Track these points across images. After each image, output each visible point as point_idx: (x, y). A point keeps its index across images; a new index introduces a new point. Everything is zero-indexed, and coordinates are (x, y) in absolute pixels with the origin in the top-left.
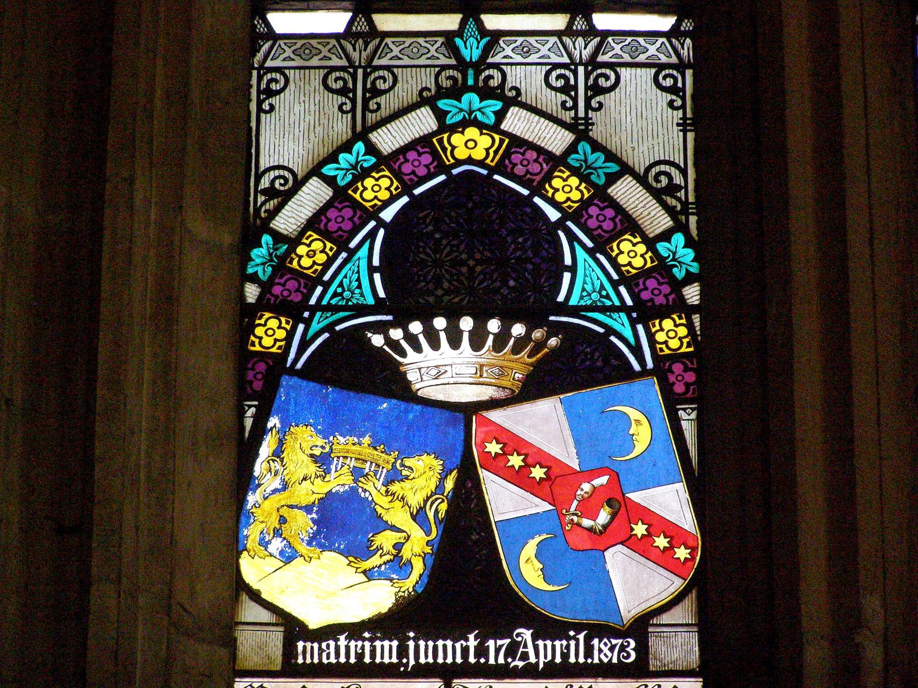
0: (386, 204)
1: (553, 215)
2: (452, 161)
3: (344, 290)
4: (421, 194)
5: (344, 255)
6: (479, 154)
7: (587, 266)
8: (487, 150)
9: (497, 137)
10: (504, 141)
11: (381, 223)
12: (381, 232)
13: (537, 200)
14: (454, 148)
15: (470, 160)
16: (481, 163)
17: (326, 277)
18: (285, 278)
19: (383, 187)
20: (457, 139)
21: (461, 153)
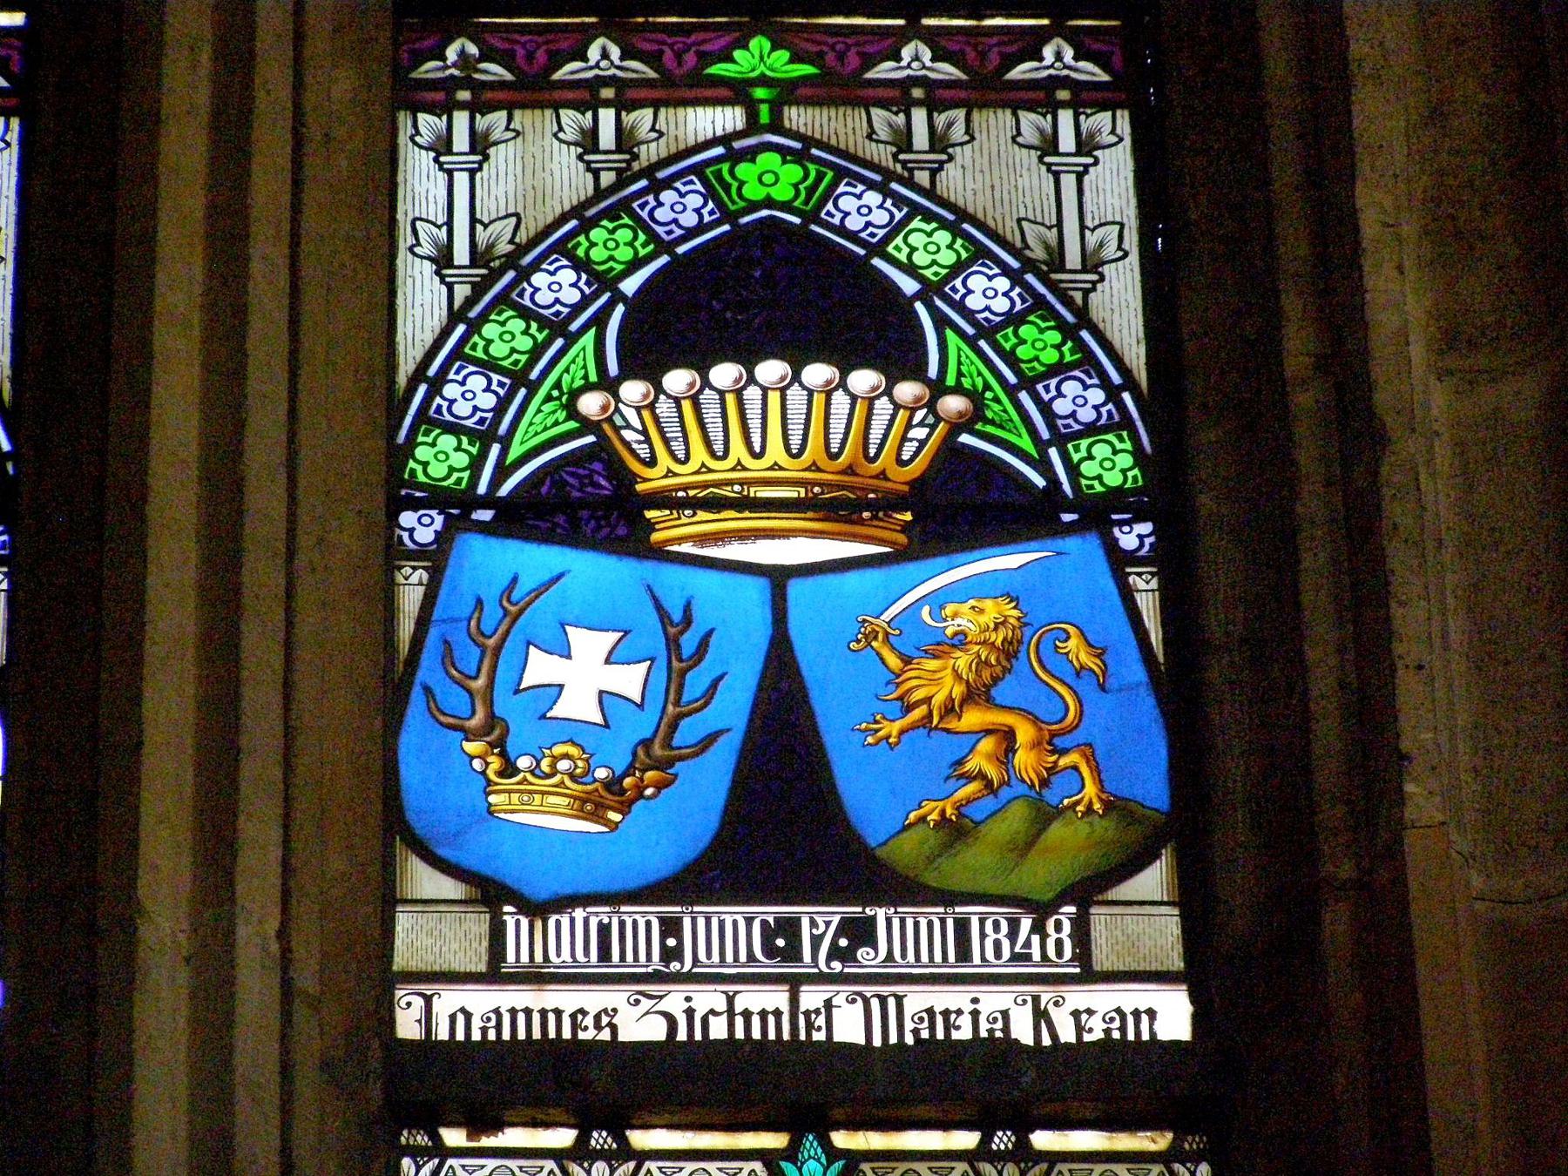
0: (635, 265)
1: (909, 286)
2: (742, 204)
3: (562, 394)
4: (685, 253)
5: (559, 342)
6: (783, 193)
7: (963, 359)
8: (796, 186)
9: (812, 168)
10: (825, 174)
11: (618, 297)
12: (620, 309)
13: (877, 262)
14: (742, 184)
15: (769, 203)
16: (786, 206)
17: (534, 375)
18: (464, 372)
19: (667, 207)
20: (743, 170)
21: (754, 192)
